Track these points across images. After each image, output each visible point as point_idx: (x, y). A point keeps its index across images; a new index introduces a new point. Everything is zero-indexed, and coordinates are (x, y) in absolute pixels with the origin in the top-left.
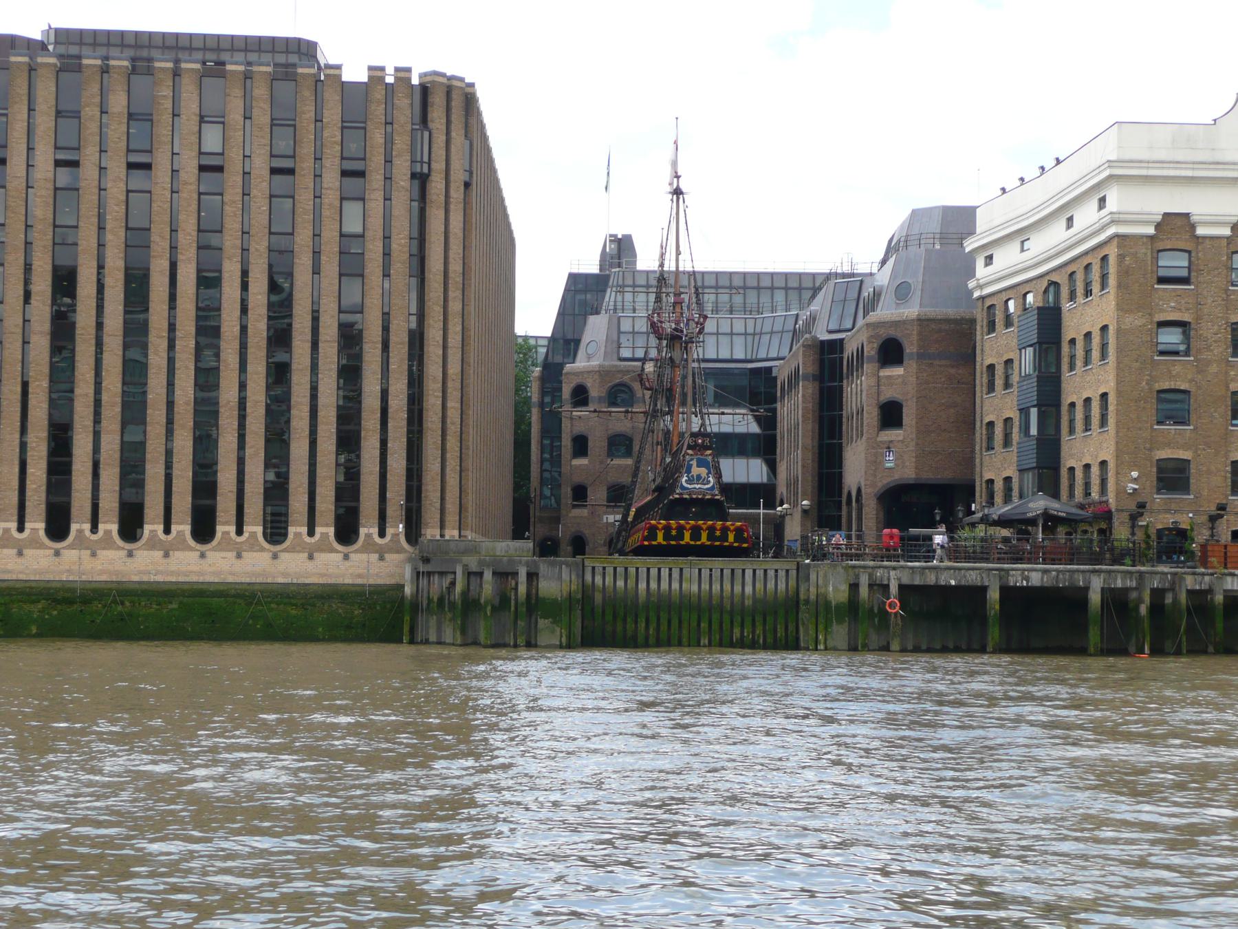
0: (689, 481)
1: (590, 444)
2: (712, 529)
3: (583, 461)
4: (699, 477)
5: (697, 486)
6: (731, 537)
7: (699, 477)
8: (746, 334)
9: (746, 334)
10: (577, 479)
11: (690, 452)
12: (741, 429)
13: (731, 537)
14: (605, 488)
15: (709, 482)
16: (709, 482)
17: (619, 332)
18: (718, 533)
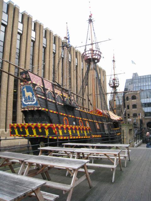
0: (26, 100)
2: (36, 127)
3: (128, 110)
4: (29, 97)
5: (30, 103)
6: (47, 132)
7: (29, 97)
10: (128, 113)
11: (22, 83)
13: (47, 132)
15: (34, 100)
16: (34, 100)
18: (40, 131)
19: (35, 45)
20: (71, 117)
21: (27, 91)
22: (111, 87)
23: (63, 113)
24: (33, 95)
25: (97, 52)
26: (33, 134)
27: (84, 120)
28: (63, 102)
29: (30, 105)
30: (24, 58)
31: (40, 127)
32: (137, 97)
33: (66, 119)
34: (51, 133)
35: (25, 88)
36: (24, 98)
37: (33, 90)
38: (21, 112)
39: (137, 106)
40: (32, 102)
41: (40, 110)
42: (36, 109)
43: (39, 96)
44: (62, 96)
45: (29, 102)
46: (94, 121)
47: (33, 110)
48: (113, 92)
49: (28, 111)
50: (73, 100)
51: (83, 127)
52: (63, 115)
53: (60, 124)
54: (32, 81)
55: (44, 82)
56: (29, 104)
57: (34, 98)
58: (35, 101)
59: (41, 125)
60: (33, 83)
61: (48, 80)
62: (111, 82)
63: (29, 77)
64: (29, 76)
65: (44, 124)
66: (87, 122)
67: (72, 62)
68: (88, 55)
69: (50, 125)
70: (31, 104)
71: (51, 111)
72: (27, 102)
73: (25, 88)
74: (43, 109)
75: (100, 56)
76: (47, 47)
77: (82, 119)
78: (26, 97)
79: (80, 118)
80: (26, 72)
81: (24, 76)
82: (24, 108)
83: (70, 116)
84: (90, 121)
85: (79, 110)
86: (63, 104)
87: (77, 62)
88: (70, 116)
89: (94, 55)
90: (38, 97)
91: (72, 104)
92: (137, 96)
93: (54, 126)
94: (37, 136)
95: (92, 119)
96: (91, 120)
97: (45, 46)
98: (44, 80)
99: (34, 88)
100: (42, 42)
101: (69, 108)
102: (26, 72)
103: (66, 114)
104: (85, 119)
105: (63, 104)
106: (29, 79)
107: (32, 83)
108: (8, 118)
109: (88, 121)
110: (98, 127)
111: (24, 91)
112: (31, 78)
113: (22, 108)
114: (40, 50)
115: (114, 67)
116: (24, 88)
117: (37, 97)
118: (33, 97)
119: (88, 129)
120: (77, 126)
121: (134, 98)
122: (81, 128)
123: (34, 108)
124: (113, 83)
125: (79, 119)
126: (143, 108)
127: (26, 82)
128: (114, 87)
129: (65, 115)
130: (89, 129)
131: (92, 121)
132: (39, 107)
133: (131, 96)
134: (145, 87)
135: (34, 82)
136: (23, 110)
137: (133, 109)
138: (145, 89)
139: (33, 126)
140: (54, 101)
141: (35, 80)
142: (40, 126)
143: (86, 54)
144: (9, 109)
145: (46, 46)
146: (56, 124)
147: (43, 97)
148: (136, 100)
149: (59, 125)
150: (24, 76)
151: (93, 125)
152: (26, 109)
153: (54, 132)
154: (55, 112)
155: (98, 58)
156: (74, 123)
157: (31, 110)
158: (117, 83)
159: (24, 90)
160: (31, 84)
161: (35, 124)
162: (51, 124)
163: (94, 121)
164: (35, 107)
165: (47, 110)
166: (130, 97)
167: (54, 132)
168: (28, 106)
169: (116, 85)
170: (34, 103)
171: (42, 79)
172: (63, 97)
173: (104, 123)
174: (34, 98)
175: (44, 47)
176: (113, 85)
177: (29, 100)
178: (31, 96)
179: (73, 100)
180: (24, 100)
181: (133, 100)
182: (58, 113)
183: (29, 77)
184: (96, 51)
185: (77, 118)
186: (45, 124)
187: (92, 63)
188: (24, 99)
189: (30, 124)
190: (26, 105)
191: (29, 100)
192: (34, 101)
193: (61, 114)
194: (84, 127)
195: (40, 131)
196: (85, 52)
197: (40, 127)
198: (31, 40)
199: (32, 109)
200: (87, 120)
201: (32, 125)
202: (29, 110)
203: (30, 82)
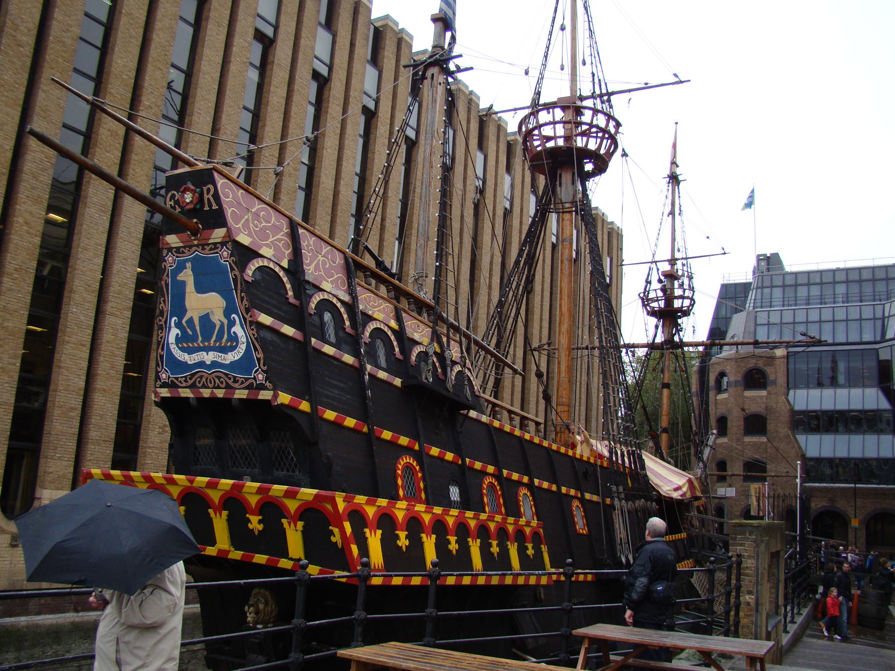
1: (729, 424)
2: (234, 504)
3: (724, 440)
4: (206, 319)
5: (209, 357)
7: (206, 319)
8: (875, 319)
9: (875, 319)
11: (172, 240)
12: (870, 405)
14: (741, 464)
17: (756, 325)
18: (255, 523)
19: (270, 59)
20: (440, 458)
21: (201, 288)
22: (653, 313)
23: (397, 430)
24: (227, 313)
25: (601, 121)
26: (213, 543)
27: (509, 479)
28: (398, 366)
29: (209, 367)
30: (210, 119)
31: (253, 500)
32: (772, 377)
33: (408, 467)
34: (318, 545)
35: (189, 265)
36: (178, 325)
37: (235, 281)
38: (156, 404)
39: (770, 426)
40: (224, 350)
41: (267, 402)
42: (241, 394)
43: (265, 319)
44: (400, 334)
45: (207, 349)
46: (564, 490)
47: (226, 402)
48: (659, 339)
49: (193, 403)
50: (454, 363)
51: (504, 520)
52: (393, 443)
53: (374, 493)
54: (229, 232)
55: (304, 244)
56: (201, 364)
57: (237, 329)
58: (243, 347)
59: (259, 491)
60: (237, 244)
61: (326, 237)
62: (655, 285)
63: (215, 207)
64: (216, 196)
65: (278, 489)
66: (523, 491)
67: (459, 169)
68: (547, 131)
69: (316, 496)
70: (215, 364)
71: (330, 415)
72: (190, 351)
73: (189, 265)
74: (284, 398)
75: (613, 139)
76: (334, 75)
77: (498, 476)
78: (191, 321)
79: (491, 469)
80: (204, 178)
81: (188, 197)
82: (172, 385)
83: (435, 451)
84: (540, 488)
85: (484, 419)
86: (398, 382)
87: (480, 174)
88: (435, 451)
89: (583, 134)
90: (260, 326)
91: (449, 385)
92: (768, 370)
93: (341, 505)
94: (236, 555)
95: (552, 481)
96: (545, 485)
97: (324, 71)
98: (301, 231)
99: (243, 269)
100: (313, 48)
101: (433, 405)
102: (204, 178)
103: (414, 436)
104: (515, 476)
105: (398, 382)
106: (218, 219)
107: (230, 241)
108: (93, 434)
109: (530, 486)
110: (580, 525)
111: (183, 284)
112: (229, 212)
113: (164, 385)
114: (296, 87)
115: (672, 213)
116: (181, 267)
117: (251, 323)
118: (232, 323)
119: (528, 530)
120: (469, 514)
121: (755, 378)
122: (492, 526)
123: (228, 387)
124: (663, 290)
125: (483, 473)
126: (801, 438)
127: (195, 232)
128: (669, 316)
129: (404, 441)
130: (535, 534)
131: (548, 491)
132: (262, 387)
133: (743, 370)
134: (841, 327)
135: (244, 239)
136: (165, 393)
137: (747, 439)
138: (844, 340)
139: (215, 496)
140: (349, 359)
141: (255, 226)
142: (258, 497)
143: (539, 127)
144: (100, 383)
145: (331, 68)
146: (351, 490)
147: (288, 330)
148: (764, 393)
149: (370, 503)
150: (188, 197)
151: (552, 509)
152: (186, 393)
153: (336, 538)
154: (350, 422)
155: (602, 151)
156: (454, 493)
157: (213, 400)
158: (682, 297)
159: (181, 277)
160: (223, 244)
161: (226, 483)
162: (323, 492)
163: (564, 490)
164: (235, 381)
165: (305, 406)
166: (733, 375)
167: (336, 538)
168: (196, 375)
169: (677, 304)
170: (231, 357)
171: (293, 226)
172: (407, 343)
173: (616, 502)
174: (237, 329)
175: (316, 75)
176: (662, 304)
177: (207, 337)
178: (218, 317)
179: (454, 363)
180: (178, 340)
181: (748, 393)
182: (365, 430)
183: (215, 207)
184: (595, 111)
185: (471, 468)
186: (285, 487)
187: (566, 178)
188: (175, 332)
189: (201, 480)
190: (184, 366)
191: (207, 338)
192: (233, 349)
193: (387, 435)
194: (511, 520)
195: (255, 523)
196: (534, 113)
197: (253, 500)
198: (251, 32)
199: (220, 393)
200: (526, 479)
201: (212, 485)
202: (201, 400)
203: (219, 234)
